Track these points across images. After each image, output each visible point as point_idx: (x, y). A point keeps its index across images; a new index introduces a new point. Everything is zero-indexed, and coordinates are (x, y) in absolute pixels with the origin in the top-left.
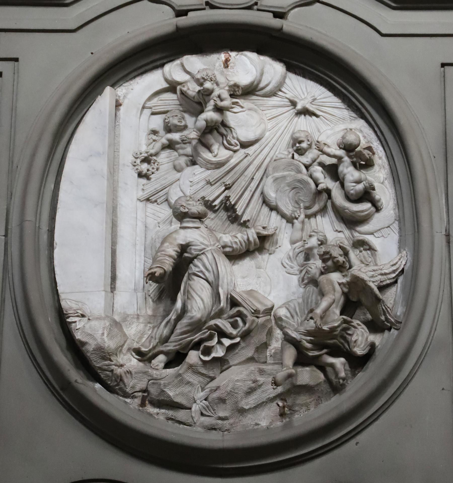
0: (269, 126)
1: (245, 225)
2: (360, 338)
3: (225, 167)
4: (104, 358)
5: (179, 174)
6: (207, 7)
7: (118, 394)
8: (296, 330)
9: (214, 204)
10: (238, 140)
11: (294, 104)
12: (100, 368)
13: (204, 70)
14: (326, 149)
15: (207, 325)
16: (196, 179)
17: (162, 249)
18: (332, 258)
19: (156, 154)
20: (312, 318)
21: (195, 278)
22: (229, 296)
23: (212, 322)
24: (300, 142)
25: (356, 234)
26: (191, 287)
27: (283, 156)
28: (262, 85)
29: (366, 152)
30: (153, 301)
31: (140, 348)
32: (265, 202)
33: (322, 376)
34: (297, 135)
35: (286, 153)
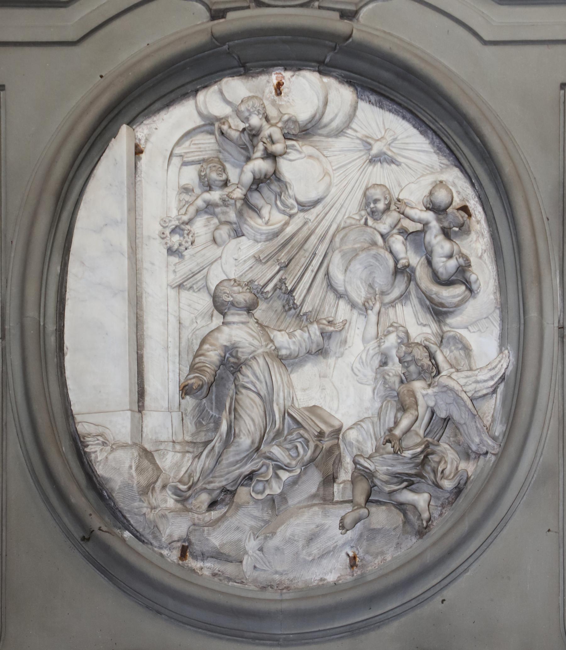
3: (279, 238)
13: (249, 98)
14: (408, 211)
17: (200, 352)
18: (415, 361)
19: (190, 222)
21: (243, 391)
27: (353, 222)
35: (357, 217)
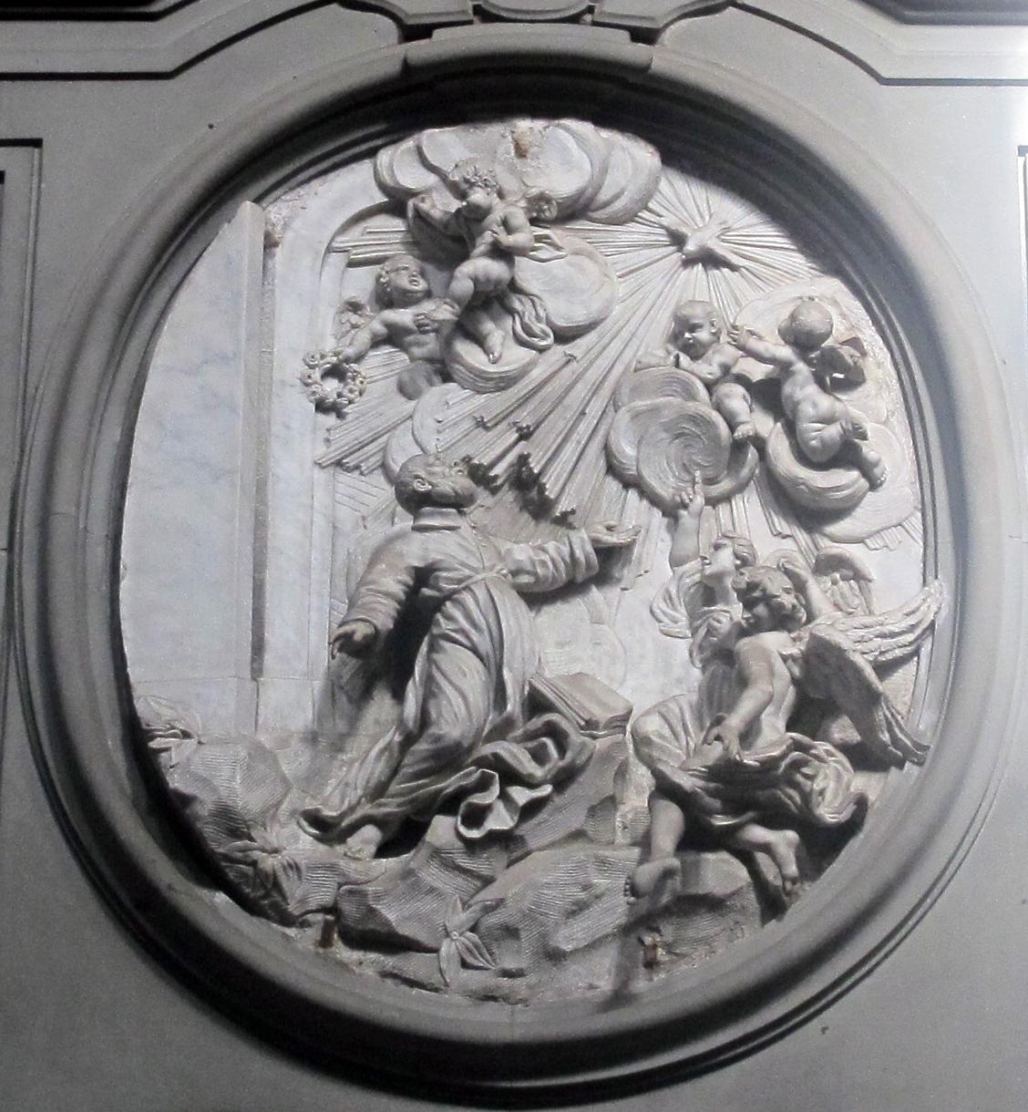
0: (622, 289)
1: (564, 521)
2: (832, 785)
4: (235, 833)
5: (413, 403)
6: (476, 19)
7: (268, 917)
8: (684, 768)
9: (492, 474)
10: (549, 323)
11: (678, 240)
12: (226, 857)
14: (753, 343)
15: (475, 755)
16: (451, 415)
17: (370, 577)
18: (767, 599)
19: (359, 358)
20: (718, 738)
21: (447, 645)
22: (527, 688)
23: (487, 750)
24: (693, 328)
25: (824, 543)
26: (438, 668)
27: (653, 361)
28: (604, 196)
29: (846, 351)
30: (350, 700)
31: (318, 810)
32: (613, 469)
33: (743, 872)
34: (687, 312)
35: (661, 353)
